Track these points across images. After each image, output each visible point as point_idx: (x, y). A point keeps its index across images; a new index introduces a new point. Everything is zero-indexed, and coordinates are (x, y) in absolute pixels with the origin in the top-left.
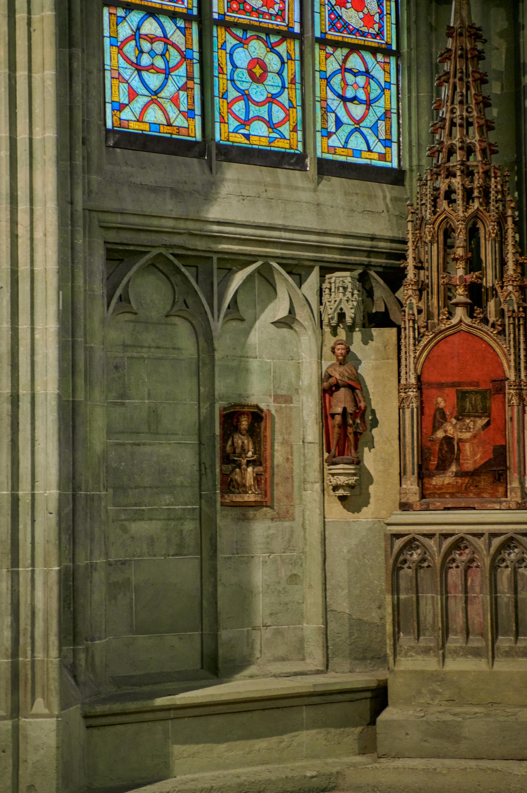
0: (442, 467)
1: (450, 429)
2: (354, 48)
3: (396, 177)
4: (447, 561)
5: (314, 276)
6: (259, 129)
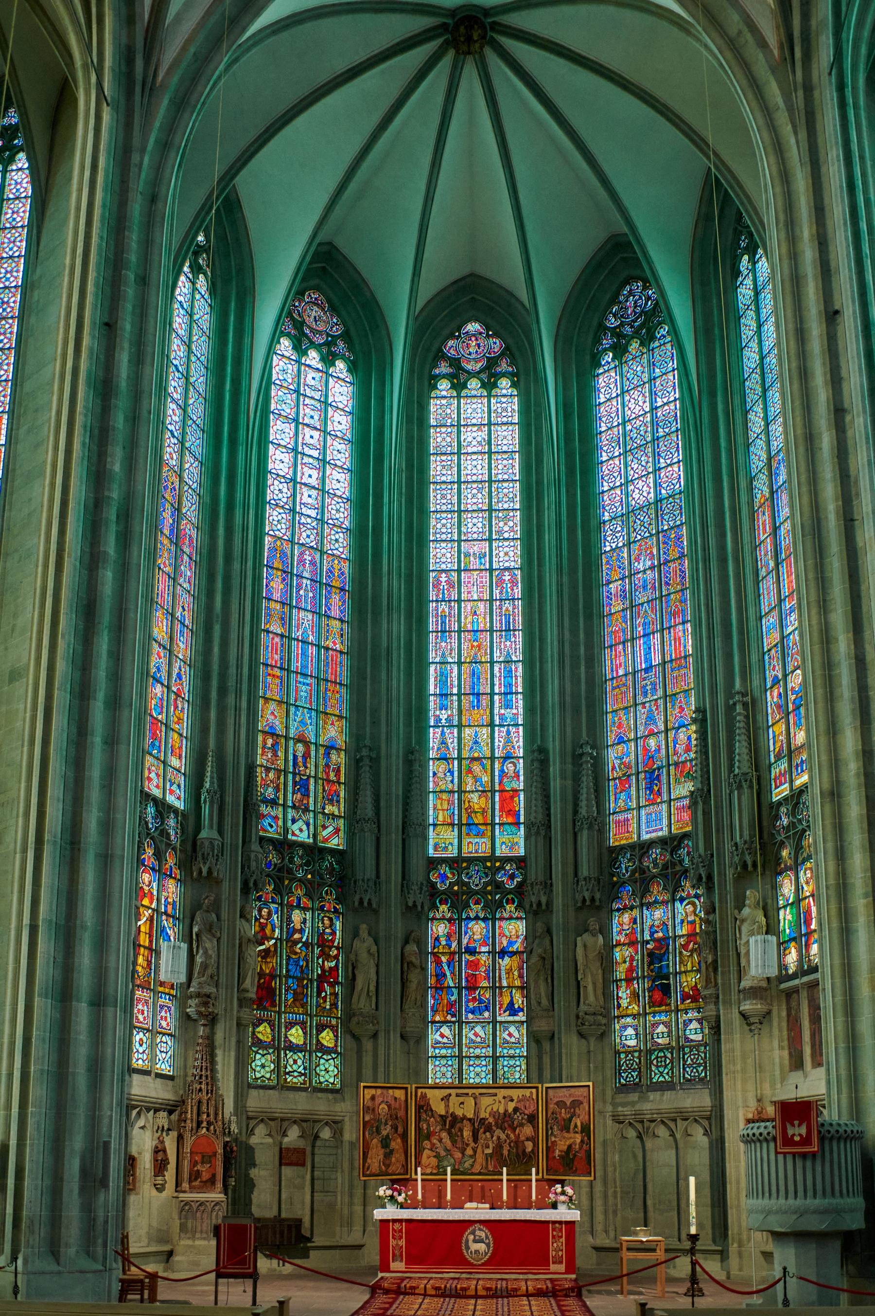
0: (196, 1179)
1: (199, 1167)
2: (164, 1034)
3: (171, 1078)
4: (213, 1210)
5: (152, 1112)
6: (140, 1062)
